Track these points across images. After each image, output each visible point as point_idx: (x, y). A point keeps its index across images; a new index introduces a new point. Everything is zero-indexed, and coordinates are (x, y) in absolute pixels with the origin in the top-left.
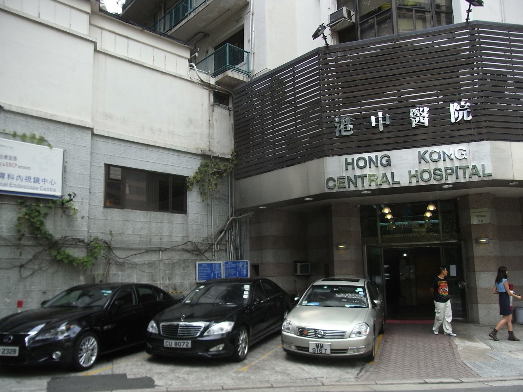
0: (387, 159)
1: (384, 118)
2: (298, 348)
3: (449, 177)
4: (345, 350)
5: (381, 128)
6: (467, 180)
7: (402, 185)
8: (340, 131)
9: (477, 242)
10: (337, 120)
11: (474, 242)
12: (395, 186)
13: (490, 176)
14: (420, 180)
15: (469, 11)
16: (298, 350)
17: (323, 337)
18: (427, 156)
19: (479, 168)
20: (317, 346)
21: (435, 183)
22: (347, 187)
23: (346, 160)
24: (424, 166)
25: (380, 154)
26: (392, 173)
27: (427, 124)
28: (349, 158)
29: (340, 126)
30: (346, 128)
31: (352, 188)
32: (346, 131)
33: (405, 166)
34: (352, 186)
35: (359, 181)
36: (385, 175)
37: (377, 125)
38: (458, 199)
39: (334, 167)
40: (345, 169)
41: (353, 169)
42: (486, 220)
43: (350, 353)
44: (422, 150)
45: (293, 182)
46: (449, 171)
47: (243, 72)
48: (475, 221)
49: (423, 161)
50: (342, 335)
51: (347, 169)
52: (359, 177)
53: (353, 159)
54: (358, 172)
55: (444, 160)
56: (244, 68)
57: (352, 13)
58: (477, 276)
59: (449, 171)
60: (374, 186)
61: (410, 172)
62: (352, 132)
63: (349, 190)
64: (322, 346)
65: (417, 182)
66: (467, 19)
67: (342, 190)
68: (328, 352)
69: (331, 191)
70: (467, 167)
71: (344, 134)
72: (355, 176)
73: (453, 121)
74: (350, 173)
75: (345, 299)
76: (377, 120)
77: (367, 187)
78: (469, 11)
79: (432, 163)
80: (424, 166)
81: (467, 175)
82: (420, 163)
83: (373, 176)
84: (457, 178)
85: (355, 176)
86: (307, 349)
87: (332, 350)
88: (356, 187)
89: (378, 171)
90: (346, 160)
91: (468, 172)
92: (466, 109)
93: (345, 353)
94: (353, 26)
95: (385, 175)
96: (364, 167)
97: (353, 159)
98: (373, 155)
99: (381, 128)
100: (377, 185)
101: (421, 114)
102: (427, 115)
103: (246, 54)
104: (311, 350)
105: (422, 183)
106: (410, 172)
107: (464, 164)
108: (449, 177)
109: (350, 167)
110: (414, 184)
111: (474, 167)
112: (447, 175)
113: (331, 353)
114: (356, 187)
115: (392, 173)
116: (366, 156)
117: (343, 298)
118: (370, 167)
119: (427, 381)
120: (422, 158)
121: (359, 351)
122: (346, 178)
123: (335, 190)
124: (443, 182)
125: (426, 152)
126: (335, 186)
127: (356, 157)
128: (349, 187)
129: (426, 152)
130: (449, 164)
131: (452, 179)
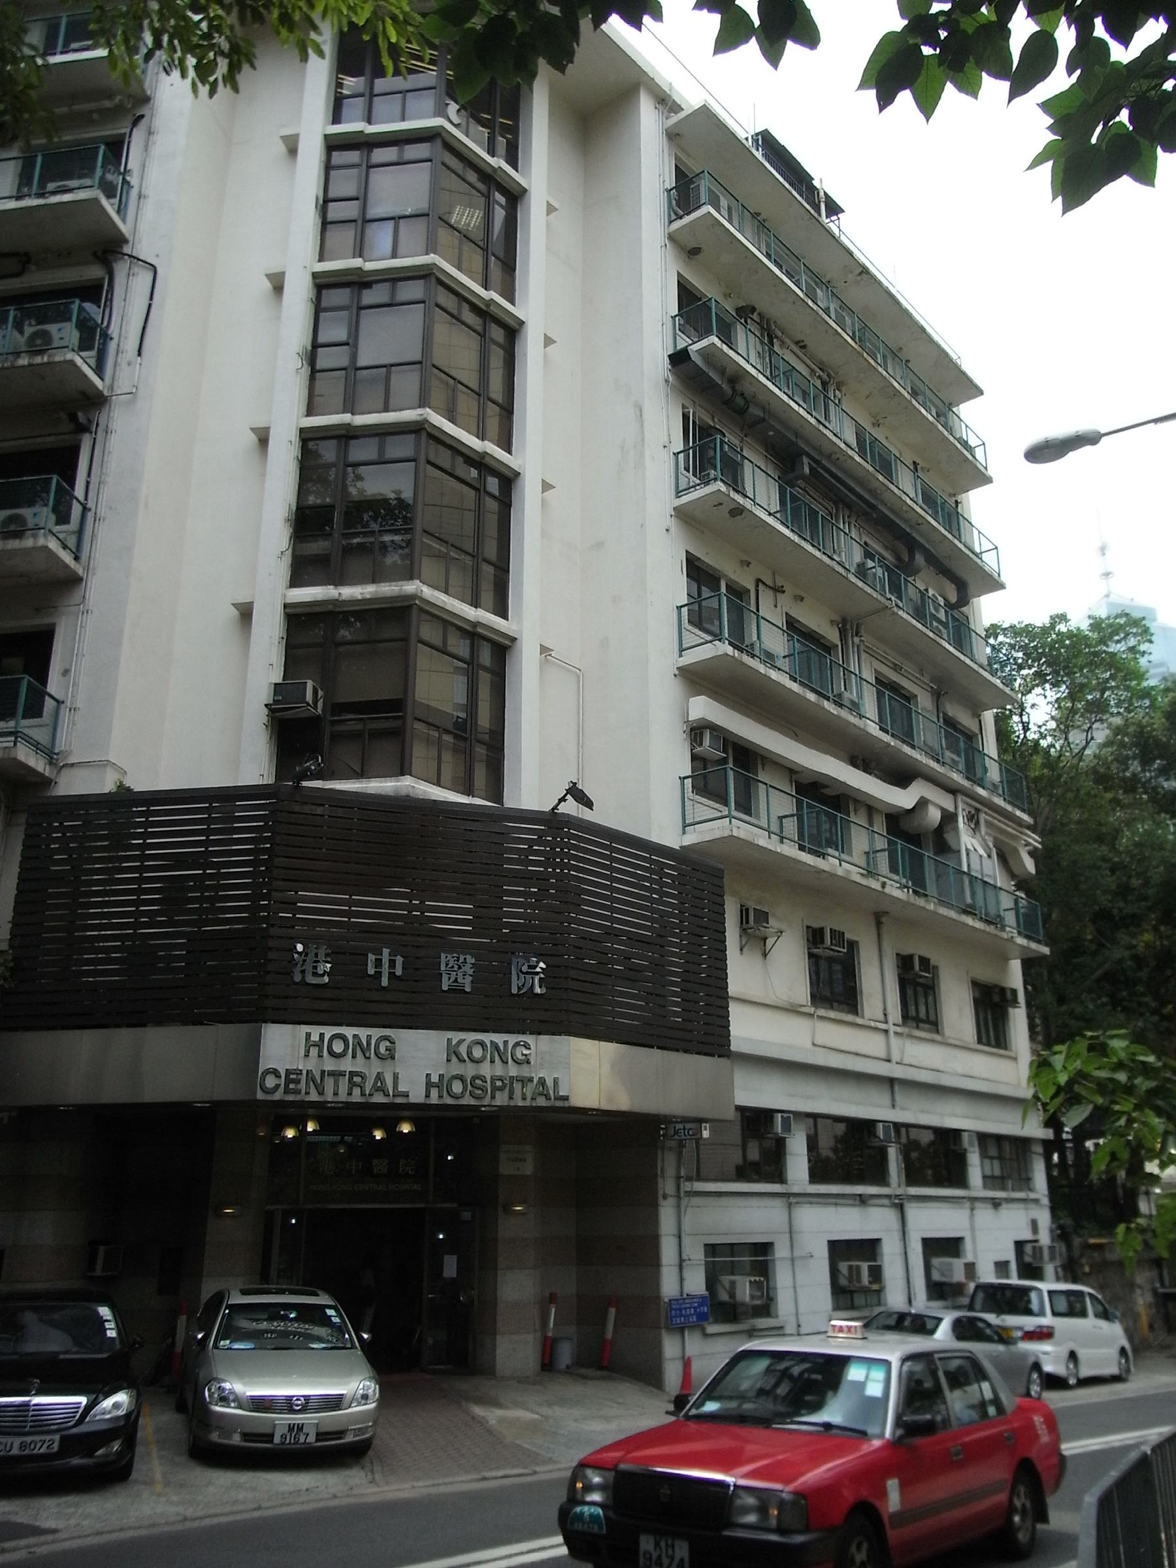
0: (388, 1044)
1: (392, 963)
2: (246, 1436)
3: (498, 1094)
4: (340, 1434)
5: (385, 982)
6: (528, 1103)
7: (414, 1099)
8: (303, 972)
9: (507, 1208)
10: (300, 947)
11: (500, 1209)
12: (398, 1100)
13: (566, 1098)
14: (445, 1093)
15: (563, 799)
16: (245, 1441)
17: (304, 1409)
18: (463, 1050)
19: (550, 1083)
20: (291, 1428)
21: (473, 1102)
22: (303, 1091)
23: (308, 1035)
24: (456, 1068)
25: (376, 1033)
26: (396, 1077)
27: (468, 989)
28: (315, 1032)
29: (304, 961)
30: (315, 968)
31: (314, 1096)
32: (315, 974)
33: (419, 1063)
34: (313, 1090)
35: (329, 1083)
36: (379, 1077)
37: (378, 975)
38: (476, 1120)
39: (283, 1047)
40: (302, 1053)
41: (320, 1056)
42: (528, 1169)
43: (349, 1438)
44: (456, 1036)
45: (167, 1063)
46: (499, 1083)
47: (37, 746)
48: (506, 1168)
49: (454, 1059)
50: (335, 1402)
51: (306, 1056)
52: (332, 1074)
53: (322, 1035)
54: (330, 1065)
55: (492, 1061)
56: (40, 735)
57: (320, 693)
58: (499, 1279)
59: (499, 1083)
60: (357, 1097)
61: (428, 1075)
62: (326, 979)
63: (307, 1099)
64: (300, 1428)
65: (440, 1097)
66: (555, 808)
67: (291, 1098)
68: (312, 1439)
69: (269, 1097)
70: (531, 1080)
71: (311, 979)
72: (323, 1072)
73: (514, 991)
74: (311, 1064)
75: (272, 1332)
76: (378, 963)
77: (343, 1097)
78: (563, 799)
79: (470, 1065)
80: (456, 1068)
81: (529, 1097)
82: (448, 1061)
83: (357, 1074)
84: (511, 1098)
85: (323, 1072)
86: (269, 1437)
87: (317, 1434)
88: (321, 1093)
89: (370, 1067)
90: (308, 1035)
91: (529, 1090)
92: (538, 973)
93: (340, 1438)
94: (314, 722)
95: (379, 1077)
96: (342, 1055)
97: (322, 1035)
98: (363, 1033)
99: (385, 982)
100: (363, 1094)
101: (460, 968)
102: (471, 972)
103: (49, 704)
104: (277, 1439)
105: (449, 1101)
106: (428, 1075)
107: (525, 1071)
108: (498, 1094)
109: (314, 1051)
110: (434, 1099)
111: (542, 1081)
112: (495, 1089)
113: (317, 1440)
114: (321, 1093)
115: (396, 1077)
116: (349, 1032)
117: (267, 1331)
118: (354, 1057)
119: (487, 1474)
120: (453, 1052)
121: (363, 1434)
122: (304, 1072)
123: (278, 1096)
124: (486, 1101)
125: (461, 1042)
126: (277, 1086)
127: (329, 1031)
128: (307, 1093)
129: (461, 1042)
130: (499, 1070)
131: (501, 1099)
